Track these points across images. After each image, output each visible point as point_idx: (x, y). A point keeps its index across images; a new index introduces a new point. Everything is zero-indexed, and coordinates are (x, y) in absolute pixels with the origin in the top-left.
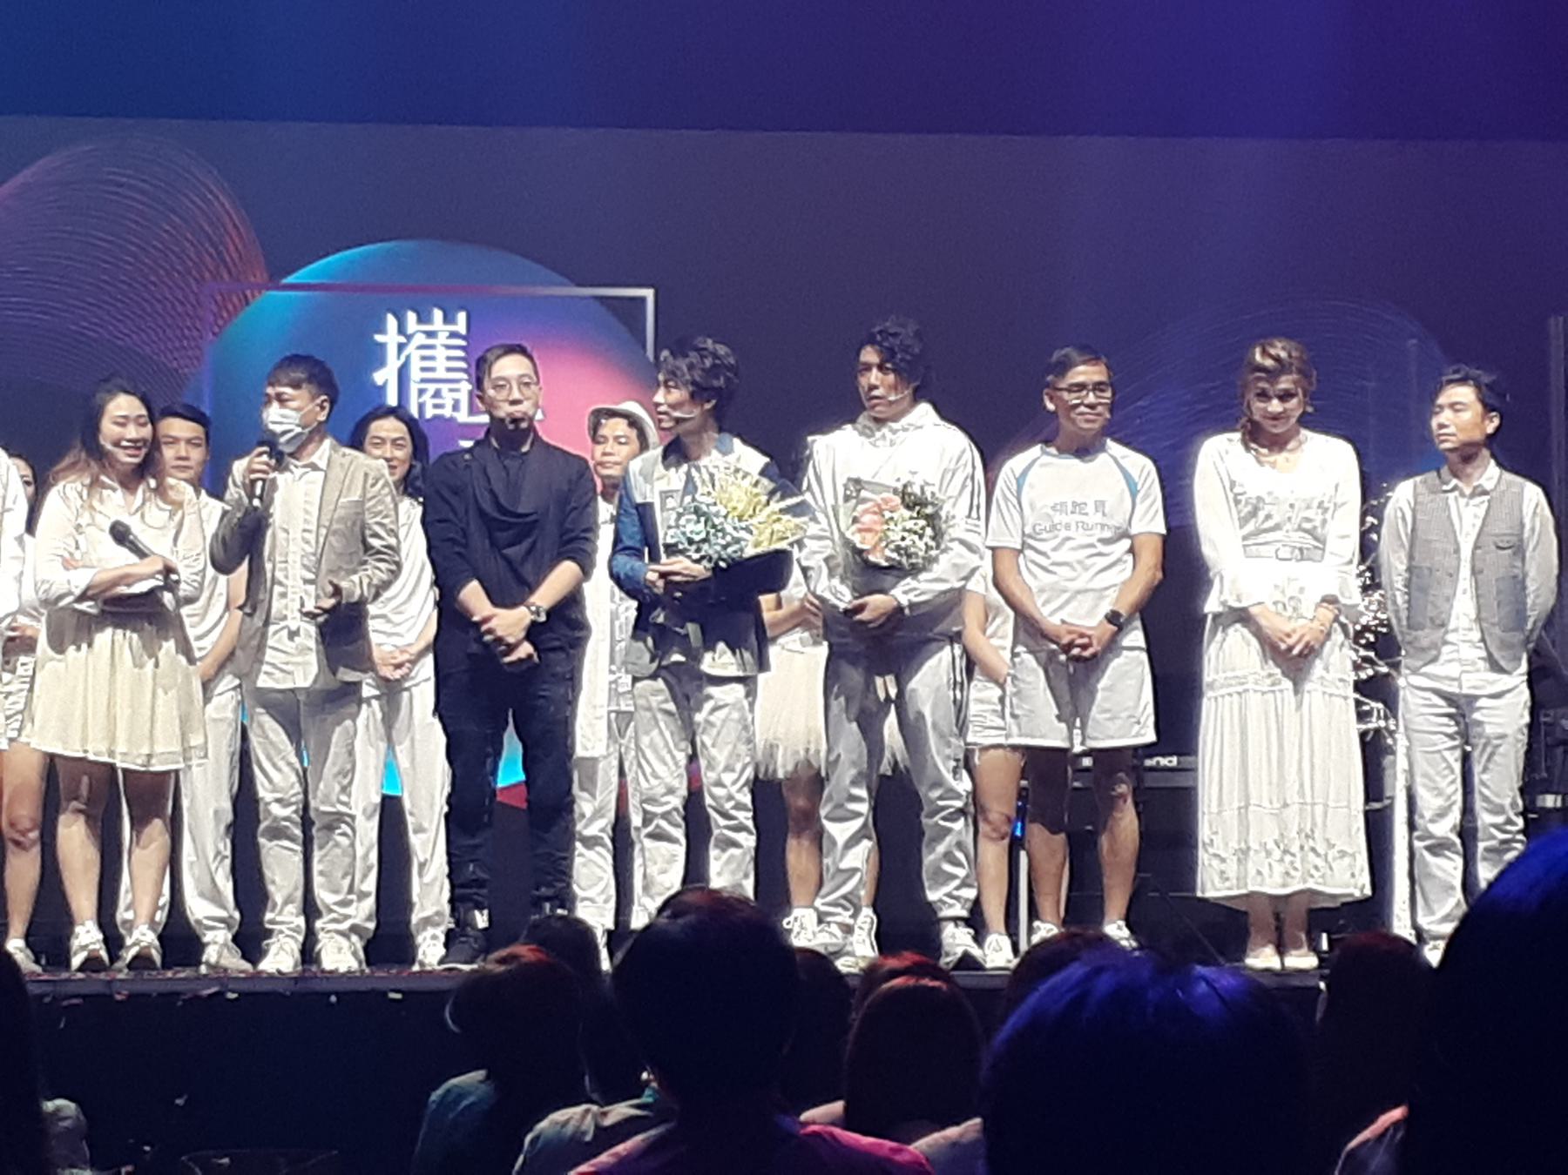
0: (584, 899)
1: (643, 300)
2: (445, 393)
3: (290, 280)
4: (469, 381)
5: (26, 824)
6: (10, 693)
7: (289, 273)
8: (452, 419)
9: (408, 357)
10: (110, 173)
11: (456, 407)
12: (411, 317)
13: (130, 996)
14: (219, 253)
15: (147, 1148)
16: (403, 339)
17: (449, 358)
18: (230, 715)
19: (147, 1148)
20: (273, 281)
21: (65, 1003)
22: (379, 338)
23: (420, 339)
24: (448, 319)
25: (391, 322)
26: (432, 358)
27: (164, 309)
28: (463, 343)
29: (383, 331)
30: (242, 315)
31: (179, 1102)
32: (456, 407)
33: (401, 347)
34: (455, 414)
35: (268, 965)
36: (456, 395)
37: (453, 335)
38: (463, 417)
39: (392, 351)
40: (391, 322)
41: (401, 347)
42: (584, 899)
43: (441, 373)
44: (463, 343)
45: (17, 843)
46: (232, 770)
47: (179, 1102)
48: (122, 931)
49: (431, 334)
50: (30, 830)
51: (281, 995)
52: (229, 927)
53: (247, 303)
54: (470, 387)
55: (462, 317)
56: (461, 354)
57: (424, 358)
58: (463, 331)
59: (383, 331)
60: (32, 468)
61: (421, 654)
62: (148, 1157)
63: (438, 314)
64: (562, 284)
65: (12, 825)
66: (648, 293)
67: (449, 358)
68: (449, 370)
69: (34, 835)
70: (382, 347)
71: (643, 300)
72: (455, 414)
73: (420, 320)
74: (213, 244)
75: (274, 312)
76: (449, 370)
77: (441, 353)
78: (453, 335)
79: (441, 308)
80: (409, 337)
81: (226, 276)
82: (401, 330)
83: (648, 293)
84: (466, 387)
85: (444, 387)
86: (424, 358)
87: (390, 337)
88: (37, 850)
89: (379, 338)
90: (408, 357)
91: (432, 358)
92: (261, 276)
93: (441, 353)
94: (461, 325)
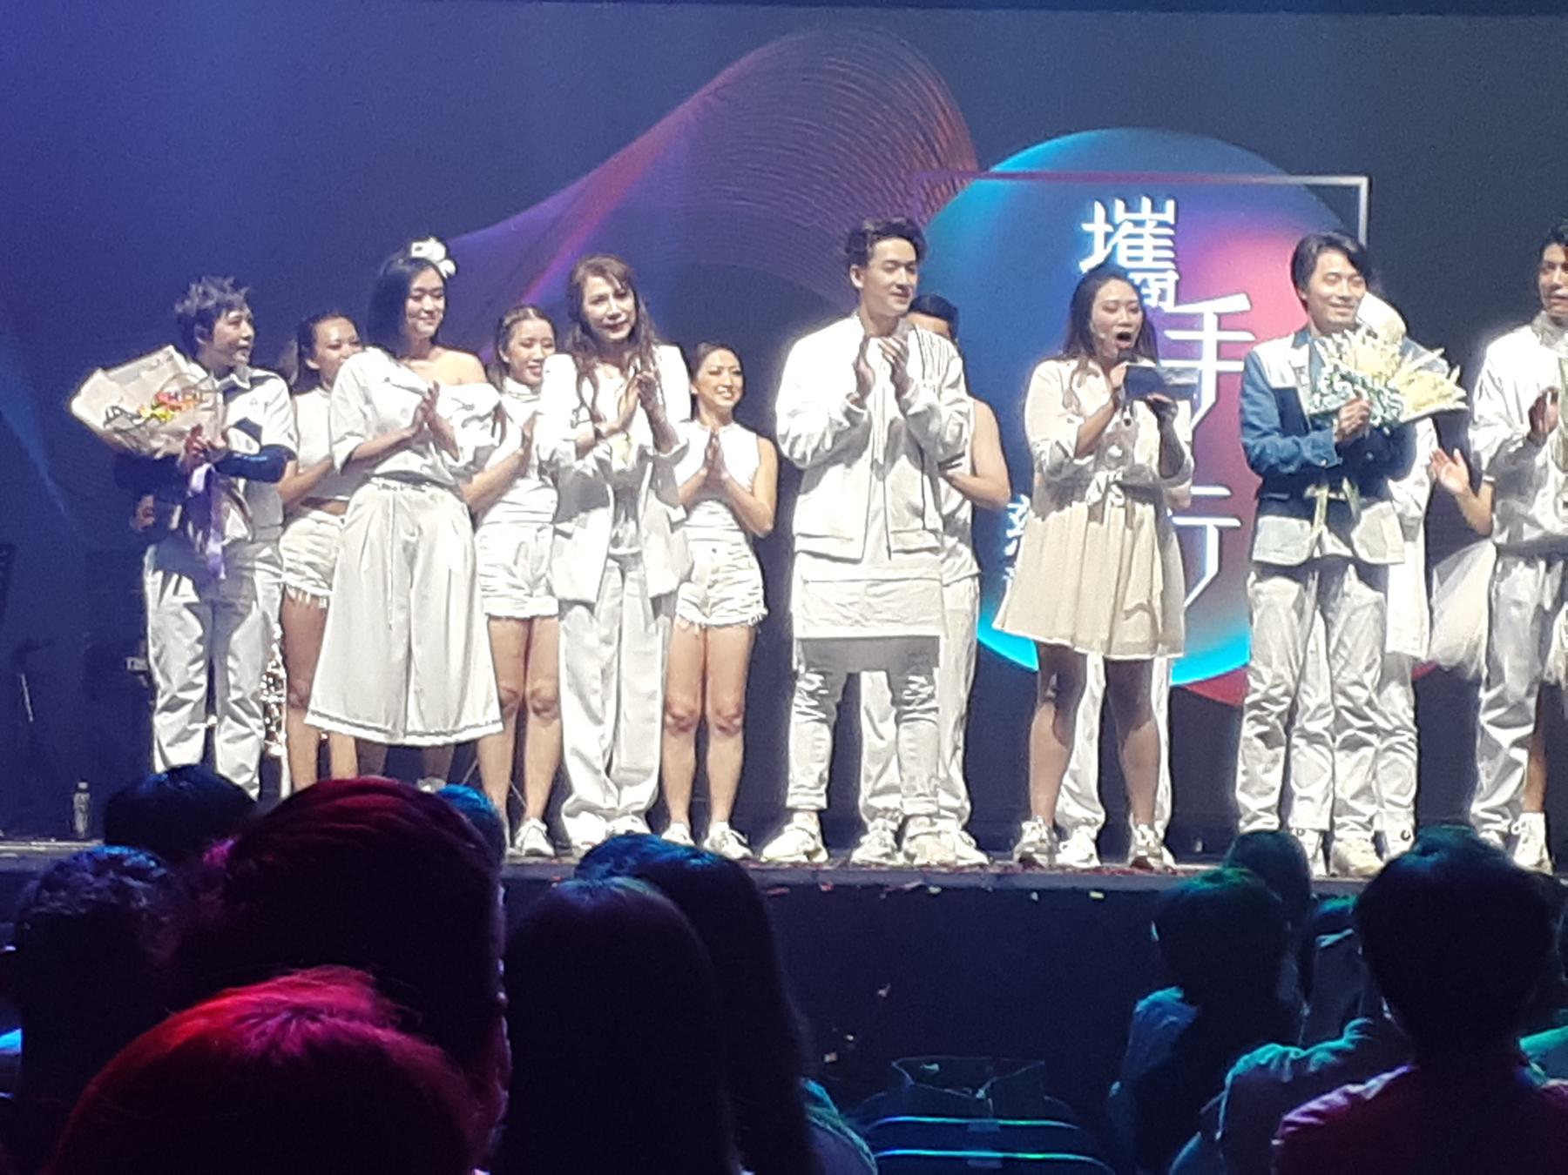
0: (1302, 798)
1: (1356, 188)
2: (1151, 282)
3: (997, 169)
4: (1177, 270)
5: (733, 711)
6: (716, 582)
7: (995, 163)
8: (1158, 309)
9: (1114, 247)
10: (830, 63)
11: (1162, 297)
12: (1119, 205)
13: (836, 886)
14: (928, 140)
15: (851, 1038)
16: (1110, 229)
17: (1156, 248)
18: (969, 608)
19: (851, 1038)
20: (983, 169)
21: (772, 892)
22: (1086, 227)
23: (1128, 228)
24: (1156, 208)
25: (1099, 209)
26: (1140, 247)
27: (893, 196)
28: (1171, 232)
29: (1091, 220)
30: (949, 204)
31: (882, 993)
32: (1162, 297)
33: (1108, 236)
34: (1162, 304)
35: (1060, 859)
36: (1162, 285)
37: (1161, 224)
38: (1169, 306)
39: (1099, 241)
40: (1099, 209)
41: (1108, 236)
42: (1302, 798)
43: (1148, 263)
44: (1171, 232)
45: (721, 728)
46: (968, 665)
47: (882, 993)
48: (865, 818)
49: (1138, 224)
50: (736, 716)
51: (985, 891)
52: (960, 818)
53: (956, 192)
54: (1176, 277)
55: (1170, 205)
56: (1169, 243)
57: (1130, 247)
58: (1172, 221)
59: (1091, 220)
60: (739, 359)
61: (1353, 551)
62: (851, 1046)
63: (1146, 203)
64: (1272, 173)
65: (718, 712)
66: (1362, 182)
67: (1156, 248)
68: (1156, 259)
69: (738, 722)
70: (1090, 235)
71: (1356, 188)
72: (1162, 304)
73: (1128, 209)
74: (924, 135)
75: (982, 200)
76: (1156, 259)
77: (1148, 242)
78: (1161, 224)
79: (1148, 196)
80: (1116, 227)
81: (935, 164)
82: (1109, 219)
83: (1362, 182)
84: (1173, 277)
85: (1151, 277)
86: (1130, 247)
87: (1097, 226)
88: (740, 736)
89: (1086, 227)
90: (1114, 247)
91: (1140, 247)
92: (972, 166)
93: (1148, 242)
94: (1169, 214)
